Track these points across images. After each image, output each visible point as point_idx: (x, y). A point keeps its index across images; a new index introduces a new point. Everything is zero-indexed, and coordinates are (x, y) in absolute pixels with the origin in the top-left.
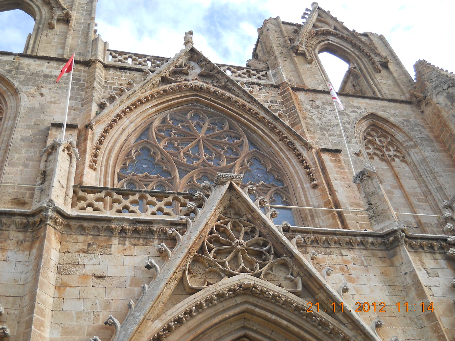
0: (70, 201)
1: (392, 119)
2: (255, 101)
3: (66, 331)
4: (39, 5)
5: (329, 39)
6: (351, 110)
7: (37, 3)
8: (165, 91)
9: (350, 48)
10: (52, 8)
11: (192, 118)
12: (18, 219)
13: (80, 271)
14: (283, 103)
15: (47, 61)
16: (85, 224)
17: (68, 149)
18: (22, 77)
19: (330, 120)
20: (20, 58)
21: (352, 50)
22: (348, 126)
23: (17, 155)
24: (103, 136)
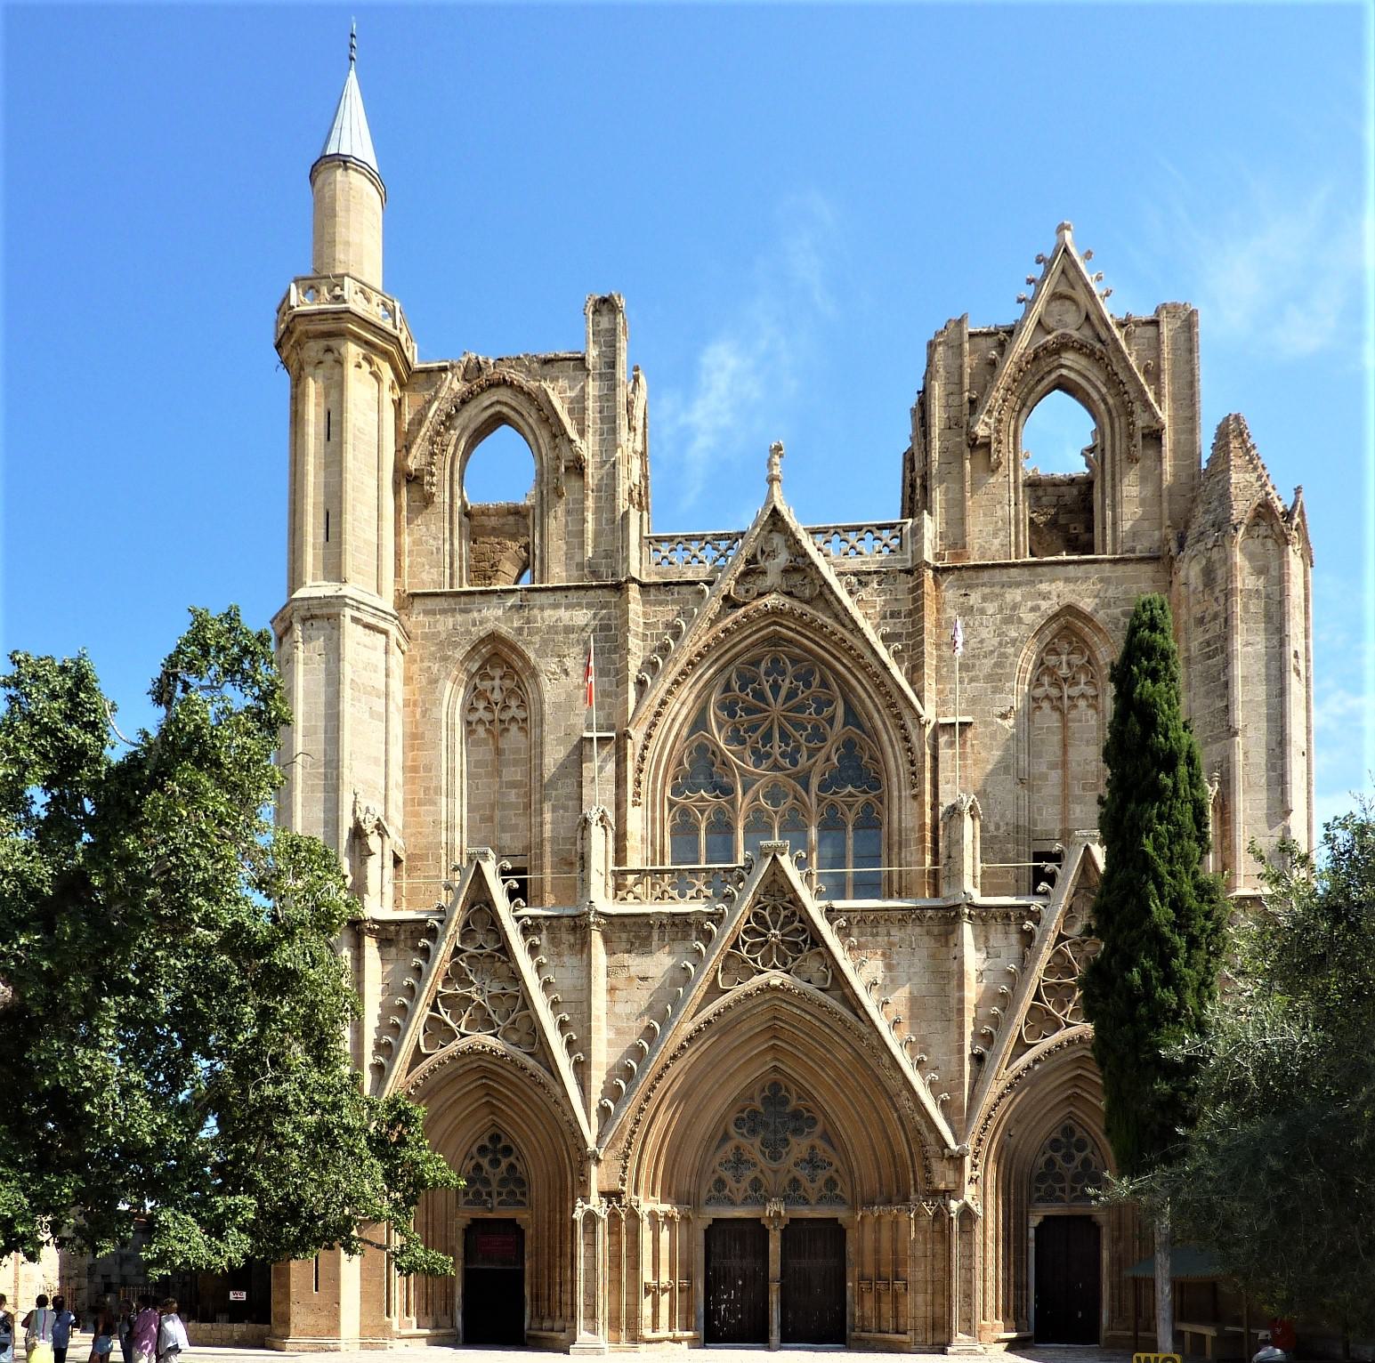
0: (611, 892)
1: (1100, 617)
2: (860, 630)
3: (619, 1032)
4: (534, 426)
5: (1063, 361)
6: (1030, 604)
7: (530, 420)
8: (726, 630)
9: (1099, 384)
10: (554, 436)
11: (768, 674)
12: (565, 921)
13: (623, 975)
14: (910, 614)
15: (564, 594)
16: (627, 920)
17: (601, 819)
18: (536, 639)
19: (981, 642)
20: (530, 596)
21: (1104, 390)
22: (1011, 650)
23: (554, 793)
24: (646, 747)
